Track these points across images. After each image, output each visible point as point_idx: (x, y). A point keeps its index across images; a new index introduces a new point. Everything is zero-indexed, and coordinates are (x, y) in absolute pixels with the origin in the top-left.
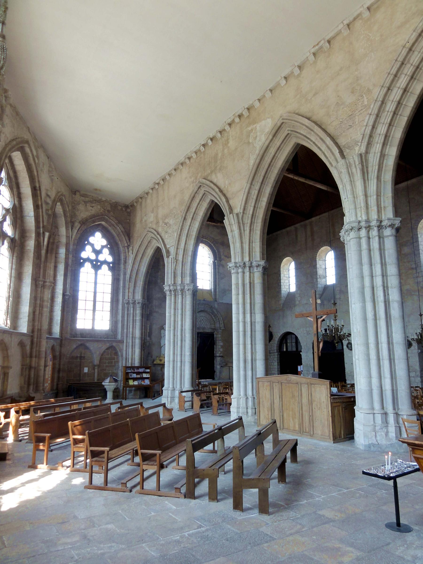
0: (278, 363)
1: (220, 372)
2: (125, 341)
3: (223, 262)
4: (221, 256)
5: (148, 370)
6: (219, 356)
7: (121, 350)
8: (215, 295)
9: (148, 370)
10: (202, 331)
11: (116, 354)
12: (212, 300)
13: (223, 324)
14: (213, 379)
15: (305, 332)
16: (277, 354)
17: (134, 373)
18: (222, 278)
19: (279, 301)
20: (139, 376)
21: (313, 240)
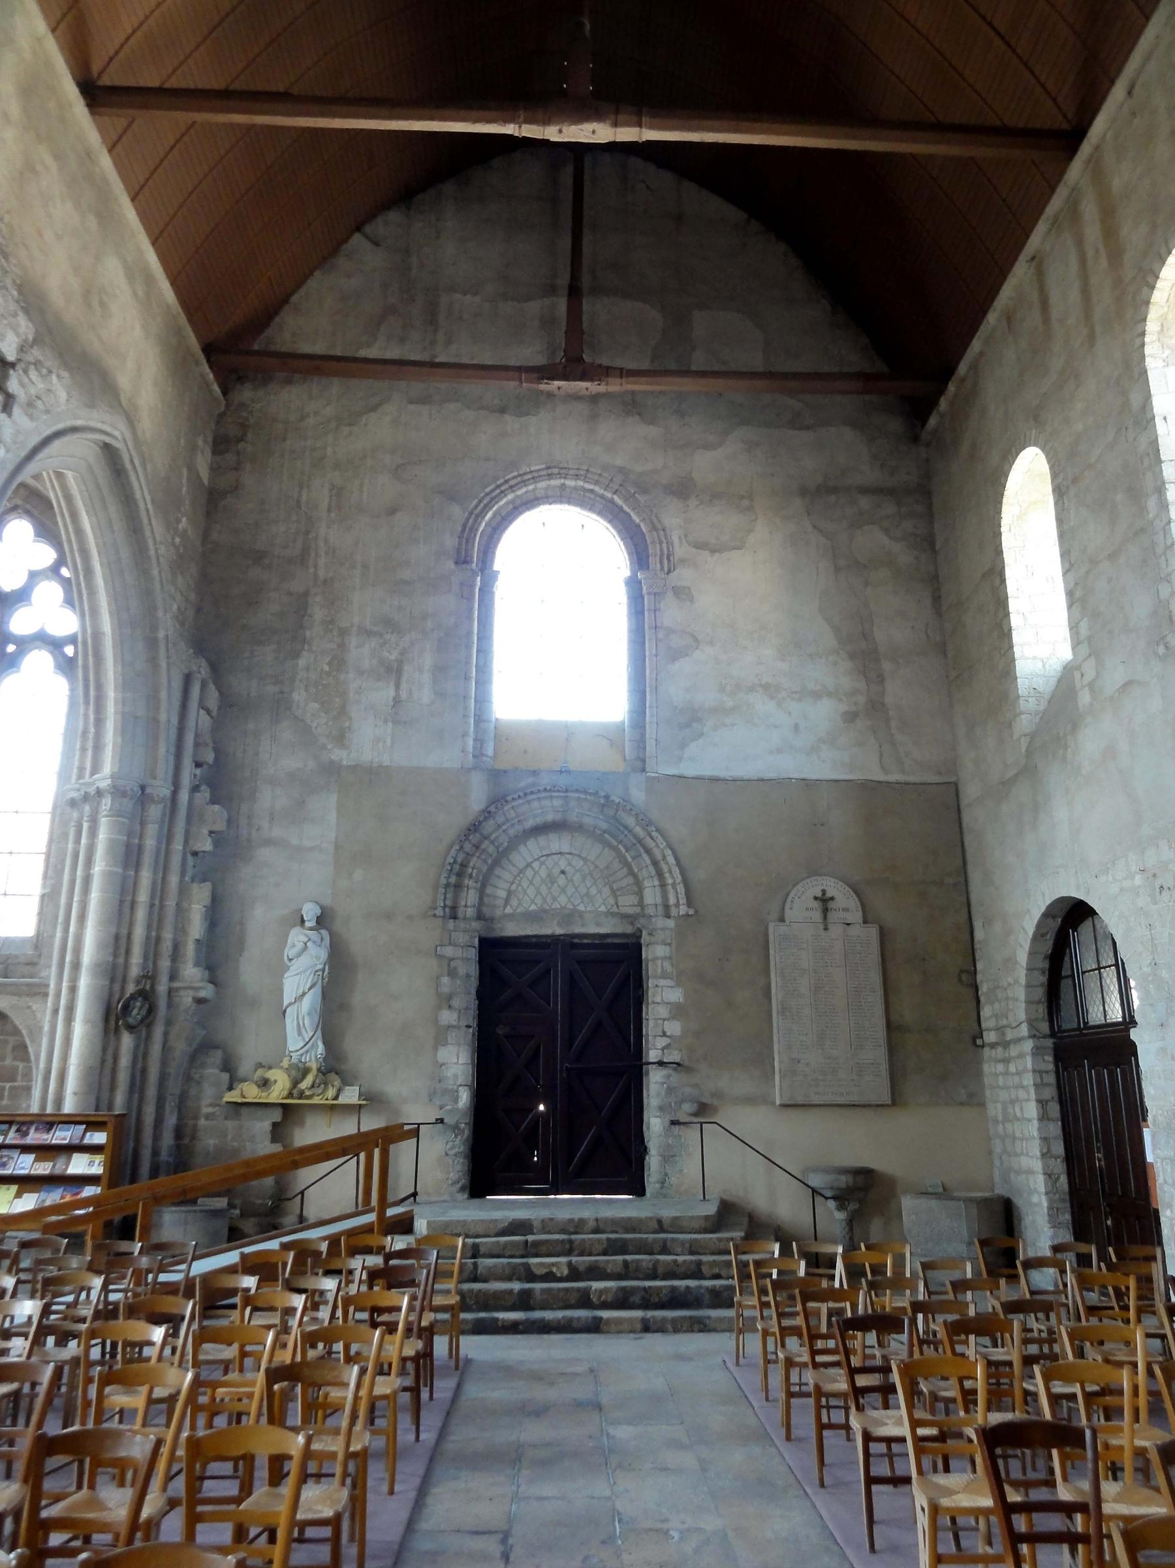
0: (1042, 1103)
1: (668, 1158)
2: (52, 986)
3: (683, 576)
4: (670, 544)
5: (99, 1138)
6: (661, 1064)
7: (36, 1032)
8: (640, 743)
9: (100, 1138)
10: (559, 931)
11: (21, 1050)
12: (621, 767)
13: (681, 889)
14: (638, 1189)
15: (1138, 880)
16: (1028, 1045)
17: (26, 1149)
18: (675, 655)
19: (1010, 726)
20: (44, 1168)
21: (1115, 254)
